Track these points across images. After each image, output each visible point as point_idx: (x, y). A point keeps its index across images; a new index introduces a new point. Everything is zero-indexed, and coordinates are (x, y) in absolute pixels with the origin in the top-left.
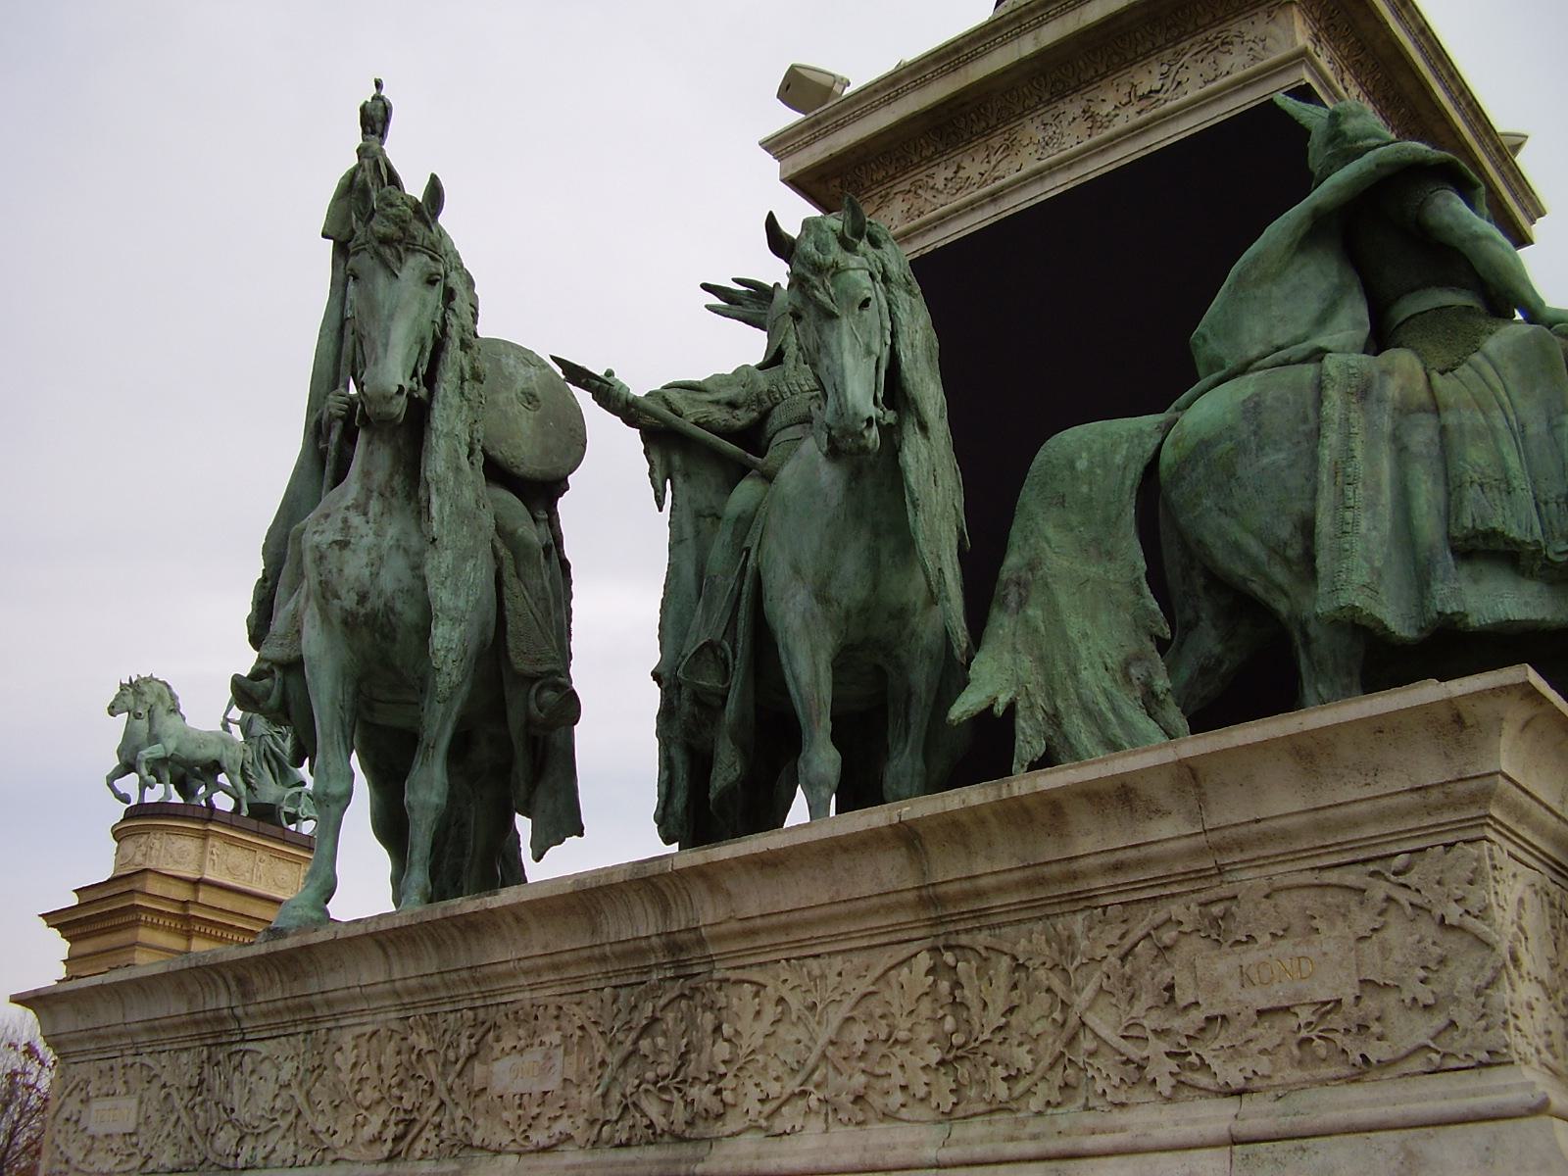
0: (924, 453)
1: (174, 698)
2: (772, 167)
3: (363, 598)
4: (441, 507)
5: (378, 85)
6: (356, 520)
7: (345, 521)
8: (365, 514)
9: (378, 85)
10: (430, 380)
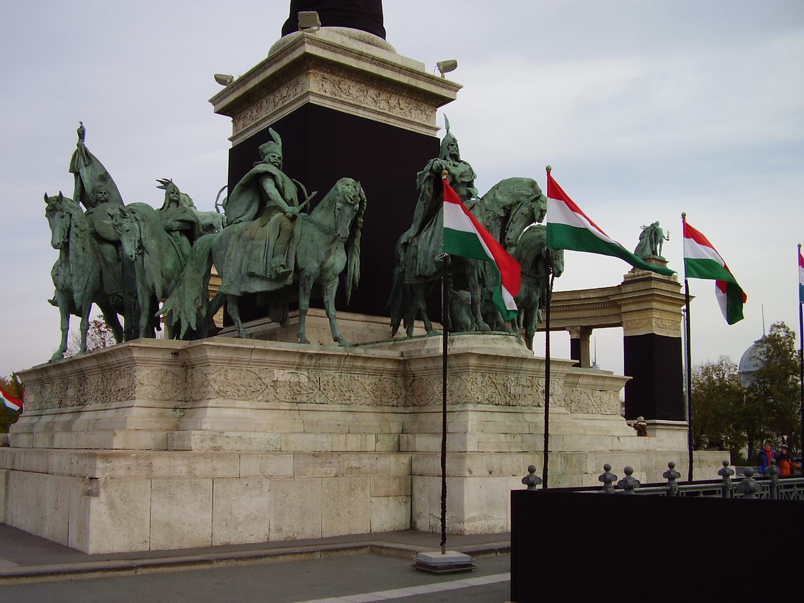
0: (148, 258)
1: (190, 200)
2: (212, 108)
3: (63, 286)
4: (73, 267)
5: (81, 123)
6: (60, 269)
7: (57, 269)
8: (61, 267)
9: (81, 123)
10: (68, 237)
